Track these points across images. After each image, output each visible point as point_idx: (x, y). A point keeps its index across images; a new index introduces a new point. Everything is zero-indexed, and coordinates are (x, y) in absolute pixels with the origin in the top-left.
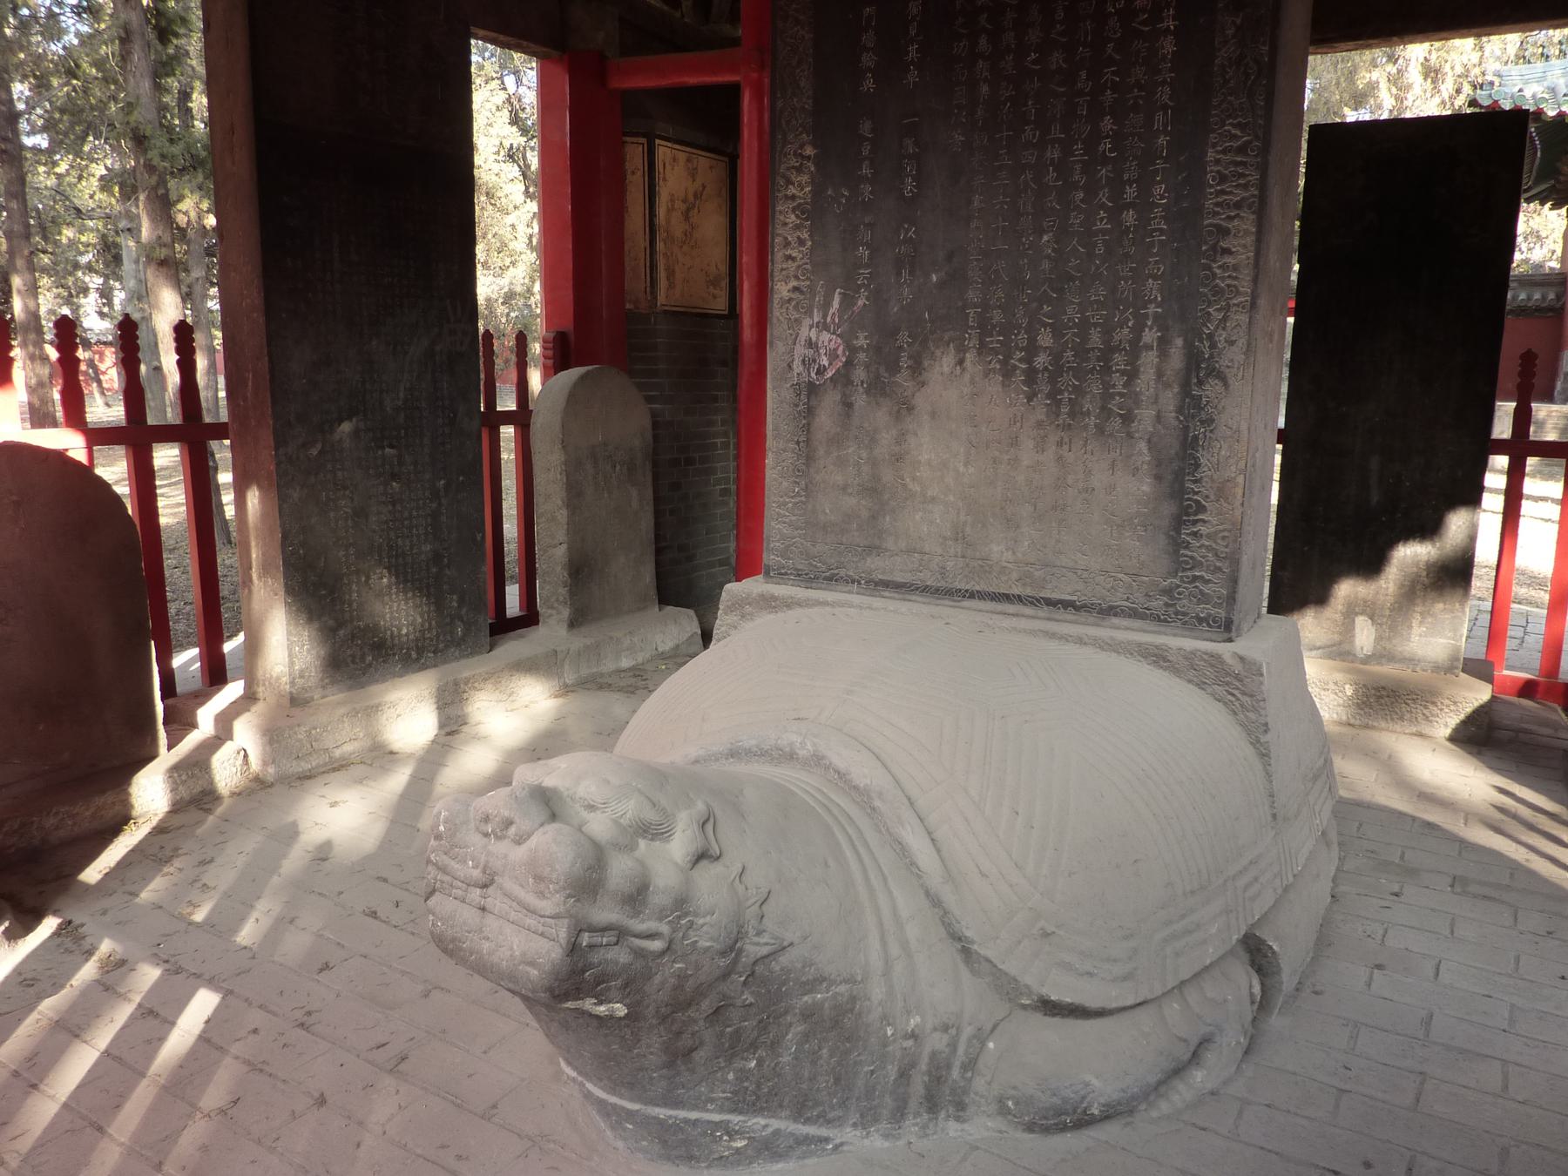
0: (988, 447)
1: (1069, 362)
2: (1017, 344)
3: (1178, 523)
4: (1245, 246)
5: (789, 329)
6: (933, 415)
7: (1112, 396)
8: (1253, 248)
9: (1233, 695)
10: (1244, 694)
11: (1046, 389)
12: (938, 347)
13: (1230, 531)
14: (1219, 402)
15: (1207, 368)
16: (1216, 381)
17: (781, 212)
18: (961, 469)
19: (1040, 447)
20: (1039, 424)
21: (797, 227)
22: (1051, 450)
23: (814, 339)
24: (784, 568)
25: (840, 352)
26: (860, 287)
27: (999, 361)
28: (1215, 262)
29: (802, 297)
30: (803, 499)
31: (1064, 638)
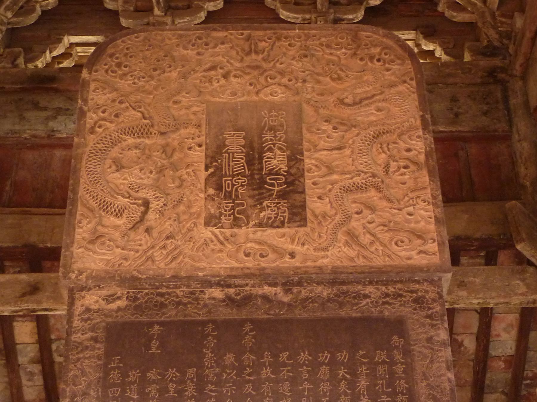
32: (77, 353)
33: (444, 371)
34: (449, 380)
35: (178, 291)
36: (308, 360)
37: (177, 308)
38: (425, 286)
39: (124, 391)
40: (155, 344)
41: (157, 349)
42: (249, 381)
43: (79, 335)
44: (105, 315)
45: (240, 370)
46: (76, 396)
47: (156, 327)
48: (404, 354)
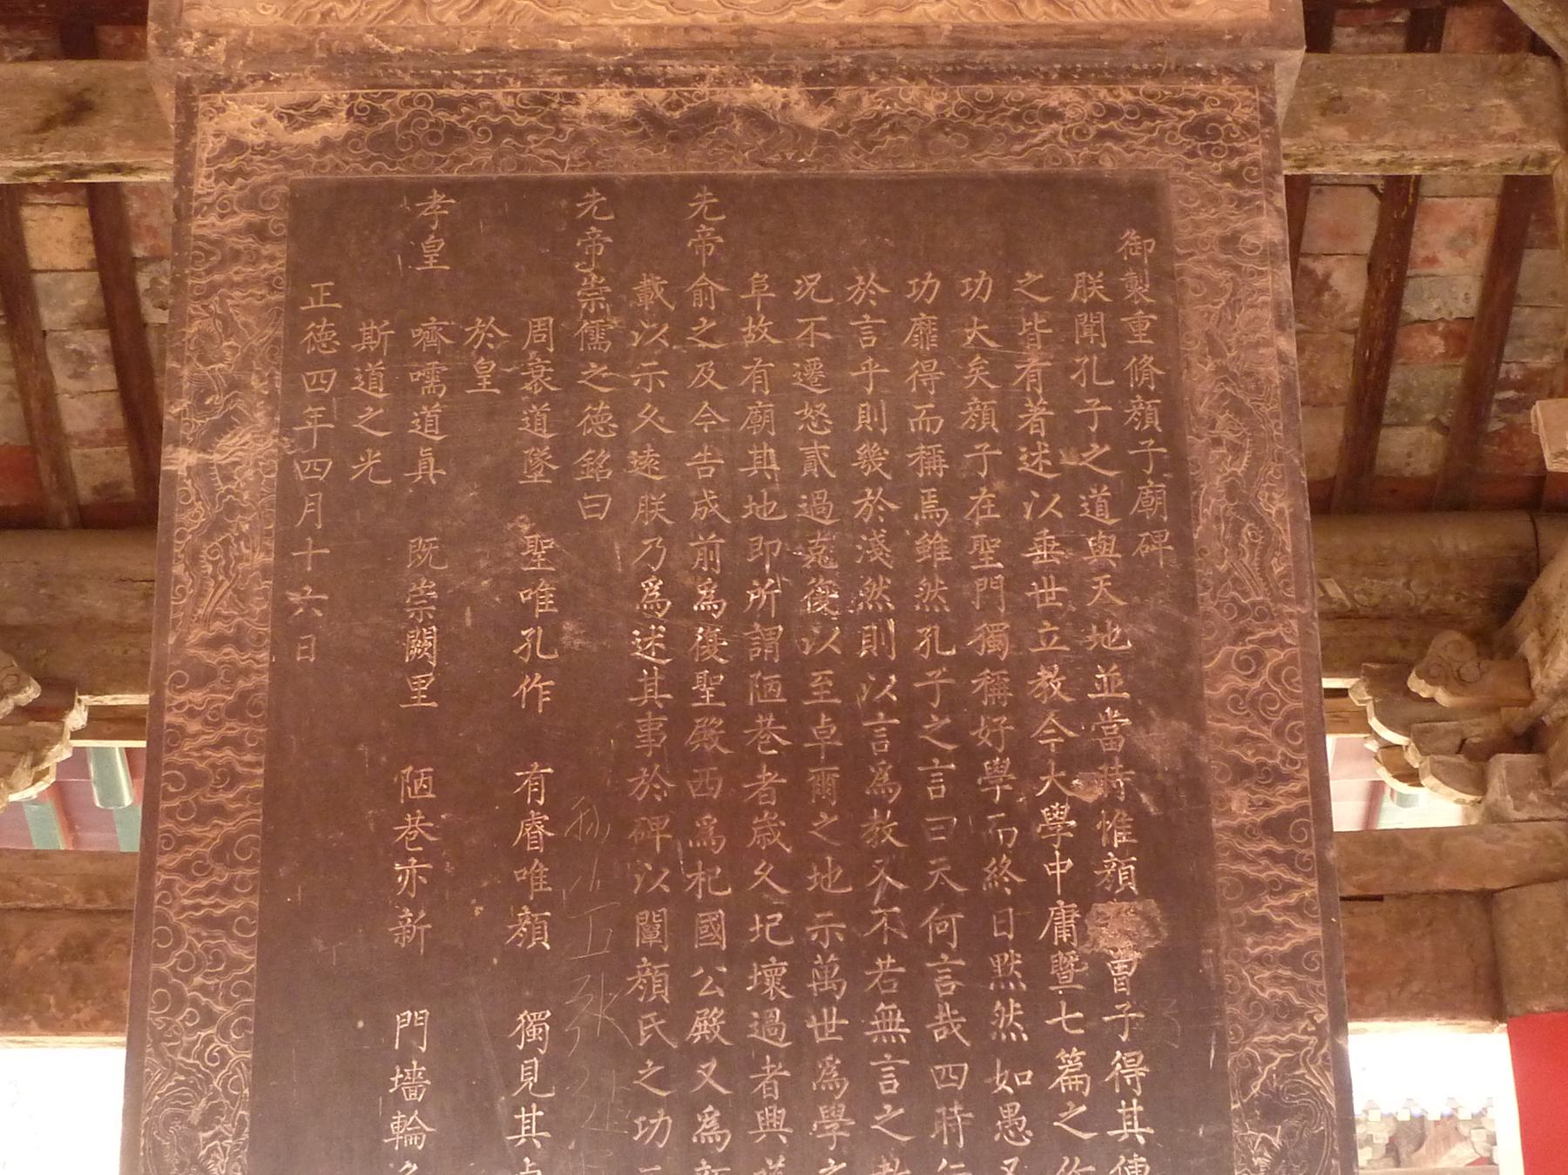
36: (878, 297)
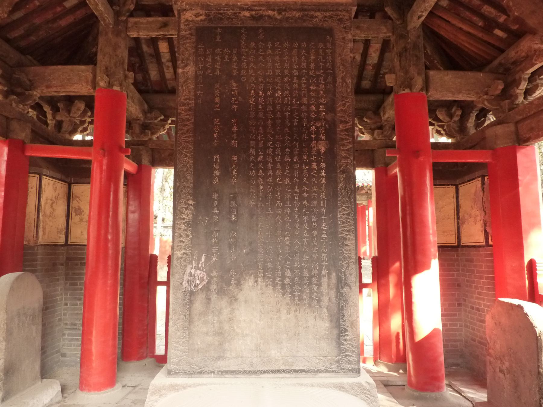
0: (268, 313)
1: (297, 281)
2: (277, 275)
3: (339, 336)
4: (352, 244)
5: (181, 269)
6: (246, 302)
7: (313, 293)
8: (354, 245)
9: (368, 397)
10: (371, 396)
11: (289, 291)
12: (247, 276)
13: (356, 337)
14: (349, 294)
15: (344, 283)
16: (347, 287)
17: (178, 224)
18: (258, 322)
19: (288, 312)
20: (287, 304)
21: (185, 230)
22: (292, 314)
23: (193, 273)
24: (178, 370)
25: (205, 278)
26: (213, 253)
27: (271, 281)
28: (343, 248)
29: (188, 257)
30: (187, 339)
31: (306, 385)
32: (183, 41)
33: (349, 53)
34: (351, 57)
35: (229, 12)
36: (288, 46)
37: (228, 20)
38: (344, 13)
39: (205, 58)
40: (218, 37)
41: (220, 39)
42: (261, 55)
43: (184, 32)
44: (195, 23)
45: (257, 50)
46: (184, 60)
47: (219, 29)
48: (331, 44)
